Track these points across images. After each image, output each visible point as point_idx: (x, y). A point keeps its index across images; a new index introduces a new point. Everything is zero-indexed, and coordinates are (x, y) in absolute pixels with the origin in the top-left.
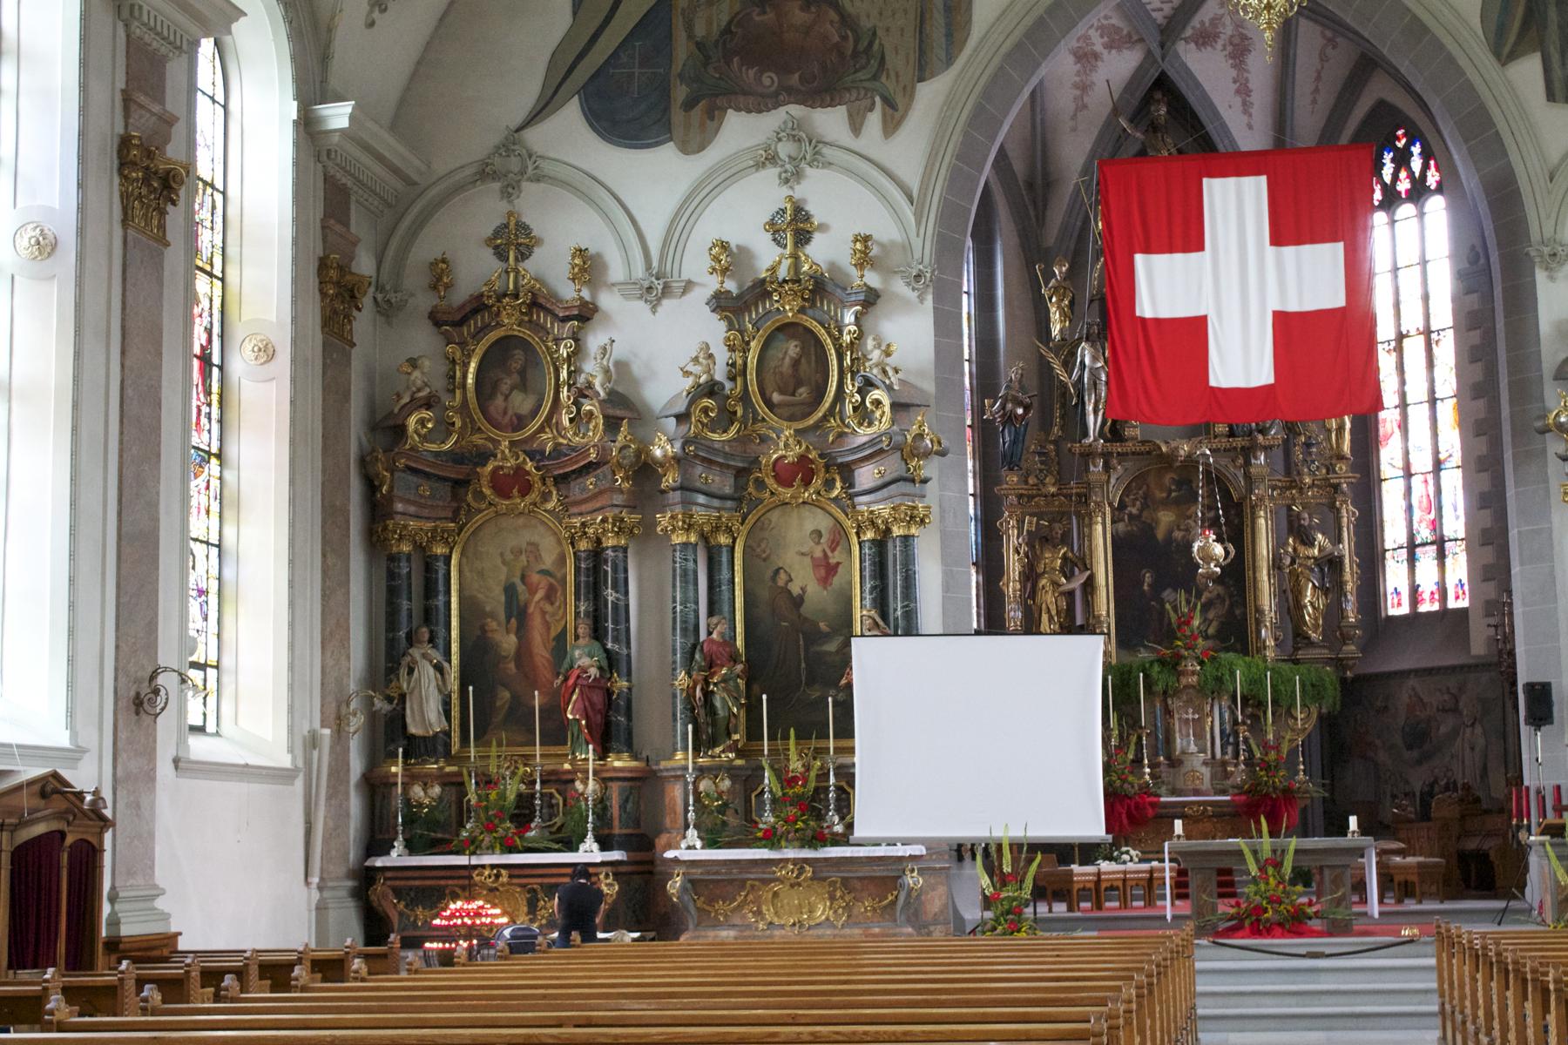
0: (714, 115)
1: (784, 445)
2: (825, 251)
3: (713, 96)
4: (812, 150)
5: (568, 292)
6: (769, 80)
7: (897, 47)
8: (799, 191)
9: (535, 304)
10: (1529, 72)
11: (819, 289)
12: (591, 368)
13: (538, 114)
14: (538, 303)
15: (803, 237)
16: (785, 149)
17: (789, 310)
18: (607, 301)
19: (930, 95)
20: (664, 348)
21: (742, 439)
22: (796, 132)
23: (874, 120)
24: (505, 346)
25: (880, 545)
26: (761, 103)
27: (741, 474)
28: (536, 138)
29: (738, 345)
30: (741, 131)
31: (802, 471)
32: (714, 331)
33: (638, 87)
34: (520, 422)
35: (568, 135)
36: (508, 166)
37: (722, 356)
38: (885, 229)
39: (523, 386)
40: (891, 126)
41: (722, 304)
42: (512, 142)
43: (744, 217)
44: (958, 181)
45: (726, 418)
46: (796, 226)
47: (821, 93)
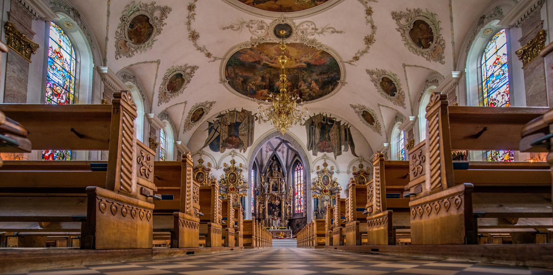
0: (225, 149)
1: (232, 186)
2: (237, 165)
3: (225, 147)
4: (235, 154)
5: (207, 167)
6: (231, 145)
7: (245, 143)
8: (234, 158)
9: (203, 169)
10: (311, 152)
11: (236, 169)
12: (209, 176)
13: (204, 147)
14: (204, 168)
15: (234, 163)
16: (232, 153)
17: (232, 171)
18: (212, 169)
19: (249, 148)
20: (218, 174)
21: (227, 185)
22: (233, 151)
23: (242, 151)
24: (200, 173)
25: (242, 198)
26: (230, 148)
27: (226, 189)
28: (204, 149)
29: (227, 175)
30: (228, 151)
31: (233, 189)
32: (224, 173)
33: (215, 144)
34: (201, 182)
35: (207, 150)
36: (200, 152)
37: (225, 176)
38: (243, 163)
39: (202, 178)
40: (244, 152)
41: (224, 170)
42: (200, 150)
43: (227, 160)
44: (251, 159)
45: (225, 183)
46: (233, 162)
47: (237, 147)
